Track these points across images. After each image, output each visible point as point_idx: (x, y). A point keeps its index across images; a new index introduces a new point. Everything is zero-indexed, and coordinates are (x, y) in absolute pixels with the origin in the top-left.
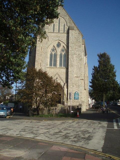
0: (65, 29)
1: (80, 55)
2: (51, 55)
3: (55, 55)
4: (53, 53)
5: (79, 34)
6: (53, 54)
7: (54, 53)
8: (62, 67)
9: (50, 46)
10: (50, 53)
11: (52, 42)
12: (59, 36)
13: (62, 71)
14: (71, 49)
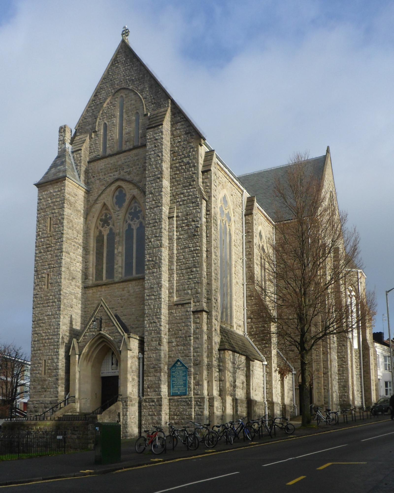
2: (99, 240)
4: (106, 232)
5: (186, 134)
8: (132, 274)
9: (93, 210)
10: (98, 233)
11: (100, 192)
12: (120, 163)
13: (132, 291)
14: (154, 200)
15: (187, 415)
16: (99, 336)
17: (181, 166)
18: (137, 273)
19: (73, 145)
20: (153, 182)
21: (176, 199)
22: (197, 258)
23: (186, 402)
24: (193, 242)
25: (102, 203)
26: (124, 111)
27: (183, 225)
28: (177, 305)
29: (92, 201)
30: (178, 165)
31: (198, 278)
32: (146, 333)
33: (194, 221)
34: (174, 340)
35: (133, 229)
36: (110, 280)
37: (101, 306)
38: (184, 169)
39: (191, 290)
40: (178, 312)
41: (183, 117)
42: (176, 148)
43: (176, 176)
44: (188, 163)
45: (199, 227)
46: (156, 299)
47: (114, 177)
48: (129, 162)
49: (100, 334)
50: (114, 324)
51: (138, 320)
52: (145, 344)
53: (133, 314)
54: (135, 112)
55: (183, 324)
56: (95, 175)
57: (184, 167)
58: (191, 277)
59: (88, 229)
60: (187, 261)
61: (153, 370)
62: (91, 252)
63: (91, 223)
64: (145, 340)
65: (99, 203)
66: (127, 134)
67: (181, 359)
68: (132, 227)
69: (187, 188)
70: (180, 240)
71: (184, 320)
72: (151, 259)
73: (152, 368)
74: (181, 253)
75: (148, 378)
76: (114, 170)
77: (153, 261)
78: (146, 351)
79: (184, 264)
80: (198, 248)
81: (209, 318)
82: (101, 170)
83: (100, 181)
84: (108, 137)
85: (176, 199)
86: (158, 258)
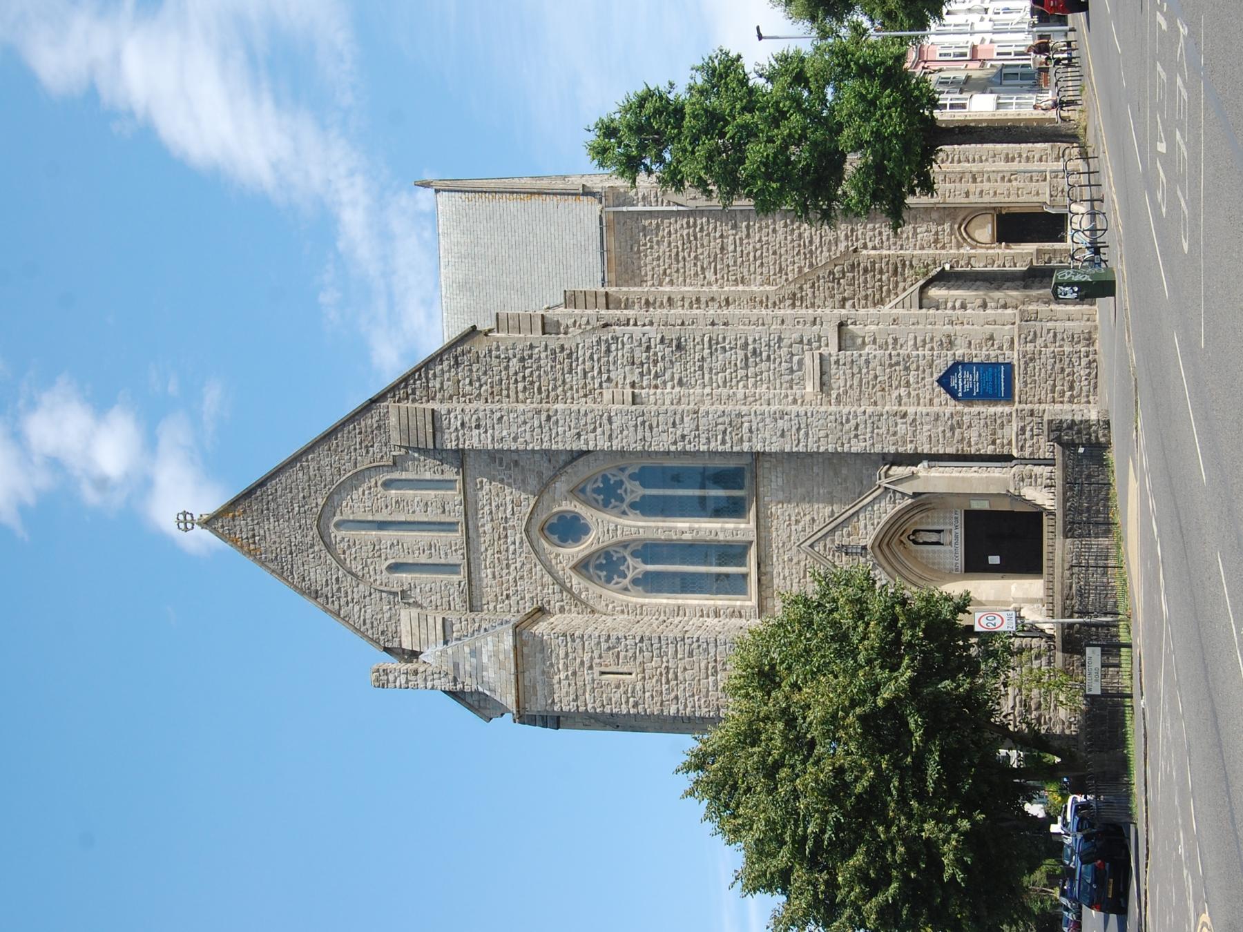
0: (428, 476)
1: (640, 355)
3: (650, 550)
6: (647, 574)
7: (630, 560)
11: (548, 579)
14: (594, 430)
15: (1055, 362)
16: (877, 549)
17: (524, 377)
18: (741, 488)
19: (424, 649)
20: (554, 432)
21: (595, 390)
22: (727, 341)
23: (1026, 364)
24: (692, 351)
25: (572, 574)
26: (370, 518)
27: (653, 372)
28: (822, 384)
29: (562, 601)
30: (520, 386)
31: (769, 340)
32: (877, 449)
33: (648, 348)
34: (895, 394)
35: (643, 497)
36: (753, 552)
37: (812, 546)
38: (532, 371)
39: (793, 355)
40: (838, 384)
41: (418, 373)
42: (484, 388)
43: (543, 388)
44: (522, 360)
45: (663, 336)
46: (807, 425)
47: (517, 544)
48: (491, 504)
49: (872, 548)
50: (853, 514)
51: (845, 480)
52: (901, 450)
53: (830, 493)
54: (380, 488)
55: (864, 371)
56: (505, 593)
57: (527, 372)
58: (765, 355)
59: (625, 611)
60: (730, 363)
61: (957, 431)
62: (680, 602)
63: (613, 602)
64: (892, 450)
65: (571, 582)
66: (426, 512)
67: (936, 376)
68: (638, 500)
69: (574, 364)
70: (685, 380)
71: (856, 370)
72: (720, 437)
73: (953, 433)
74: (711, 378)
75: (973, 443)
76: (502, 541)
77: (724, 432)
78: (916, 448)
79: (736, 371)
80: (706, 339)
81: (853, 320)
82: (494, 577)
83: (522, 578)
84: (423, 559)
85: (595, 390)
86: (721, 420)
